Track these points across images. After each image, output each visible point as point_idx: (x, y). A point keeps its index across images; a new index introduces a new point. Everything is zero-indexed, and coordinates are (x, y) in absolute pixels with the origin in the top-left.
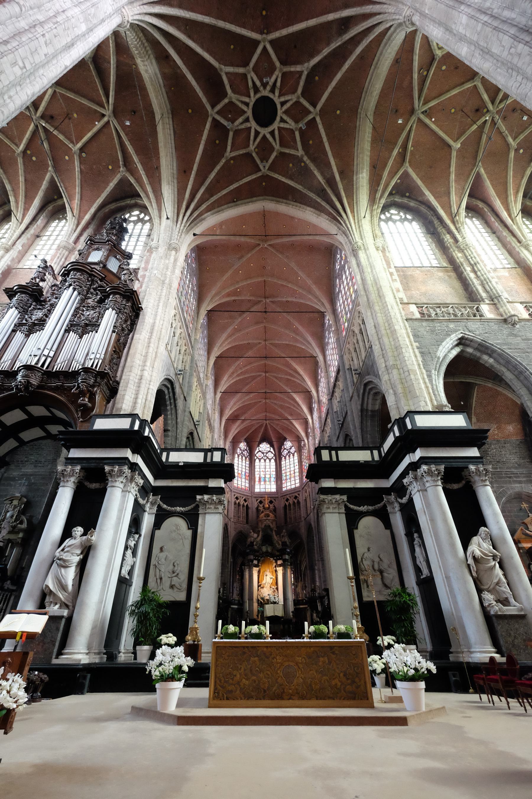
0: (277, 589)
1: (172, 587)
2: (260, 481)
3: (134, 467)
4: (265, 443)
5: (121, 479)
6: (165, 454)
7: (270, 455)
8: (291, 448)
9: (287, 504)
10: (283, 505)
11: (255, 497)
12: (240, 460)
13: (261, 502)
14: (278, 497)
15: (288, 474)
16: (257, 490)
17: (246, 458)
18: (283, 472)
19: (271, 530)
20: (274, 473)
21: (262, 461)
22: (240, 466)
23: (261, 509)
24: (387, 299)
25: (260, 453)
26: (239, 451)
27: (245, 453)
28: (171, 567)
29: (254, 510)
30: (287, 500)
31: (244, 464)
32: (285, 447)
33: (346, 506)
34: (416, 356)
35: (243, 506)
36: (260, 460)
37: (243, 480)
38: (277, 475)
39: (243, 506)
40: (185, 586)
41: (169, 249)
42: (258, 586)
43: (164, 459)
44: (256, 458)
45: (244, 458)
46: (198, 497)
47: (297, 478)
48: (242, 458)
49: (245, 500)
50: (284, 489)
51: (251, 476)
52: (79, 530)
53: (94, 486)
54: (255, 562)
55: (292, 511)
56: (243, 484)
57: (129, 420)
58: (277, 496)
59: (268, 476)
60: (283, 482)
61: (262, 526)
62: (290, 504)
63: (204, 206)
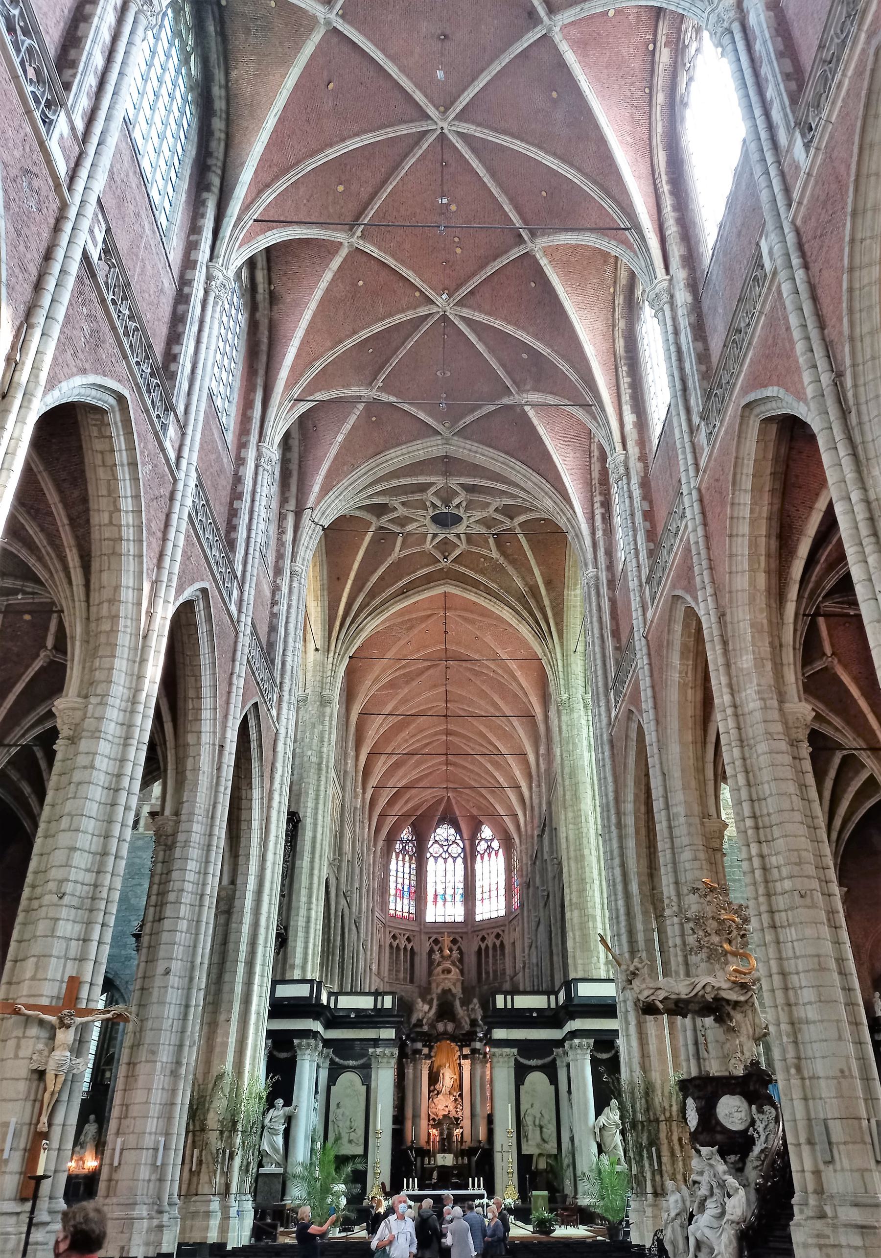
0: (461, 1095)
1: (350, 1141)
2: (435, 902)
3: (315, 1034)
4: (445, 826)
5: (308, 1052)
6: (333, 999)
7: (455, 850)
8: (492, 840)
9: (483, 946)
10: (476, 948)
11: (427, 933)
12: (400, 863)
13: (436, 941)
14: (466, 933)
15: (486, 889)
16: (430, 918)
17: (411, 859)
18: (478, 884)
19: (454, 996)
20: (461, 886)
21: (440, 860)
22: (400, 875)
23: (437, 956)
24: (583, 806)
25: (436, 846)
26: (398, 846)
27: (409, 847)
28: (348, 1123)
29: (425, 956)
30: (483, 939)
31: (407, 870)
32: (483, 836)
33: (516, 1060)
34: (602, 892)
35: (405, 948)
36: (436, 858)
37: (406, 901)
38: (466, 888)
39: (405, 948)
40: (362, 1140)
41: (321, 704)
42: (430, 1092)
43: (332, 1006)
44: (428, 855)
45: (407, 857)
46: (371, 1050)
47: (502, 900)
48: (404, 859)
49: (409, 940)
50: (478, 918)
51: (419, 893)
52: (280, 1102)
53: (283, 1055)
54: (426, 1051)
55: (491, 961)
56: (406, 909)
57: (307, 987)
58: (465, 930)
59: (450, 891)
60: (478, 903)
61: (436, 991)
62: (487, 947)
63: (362, 616)
